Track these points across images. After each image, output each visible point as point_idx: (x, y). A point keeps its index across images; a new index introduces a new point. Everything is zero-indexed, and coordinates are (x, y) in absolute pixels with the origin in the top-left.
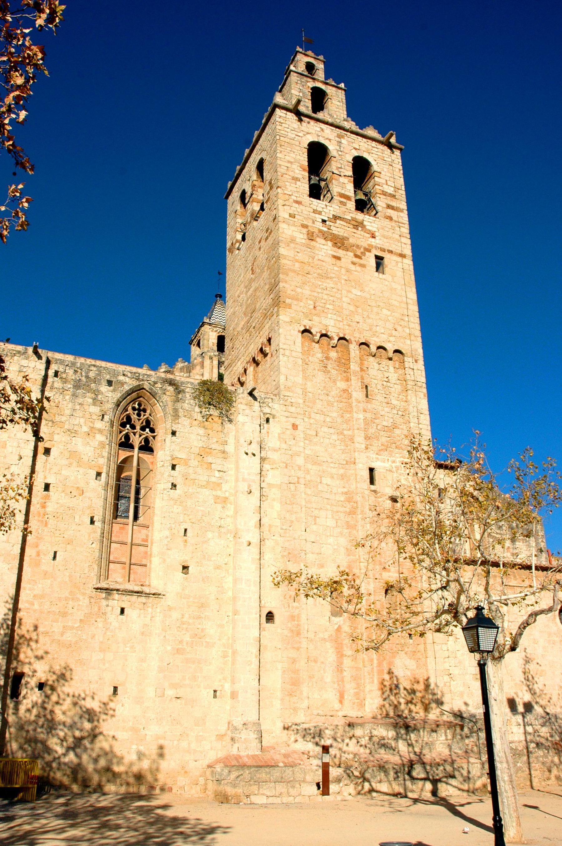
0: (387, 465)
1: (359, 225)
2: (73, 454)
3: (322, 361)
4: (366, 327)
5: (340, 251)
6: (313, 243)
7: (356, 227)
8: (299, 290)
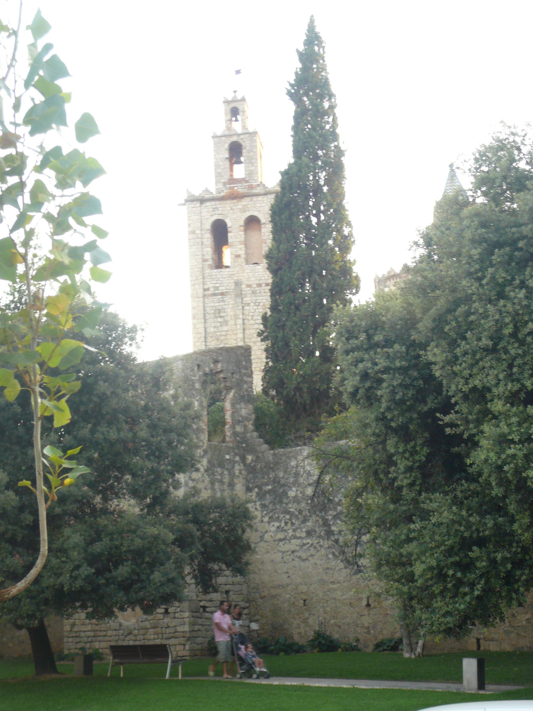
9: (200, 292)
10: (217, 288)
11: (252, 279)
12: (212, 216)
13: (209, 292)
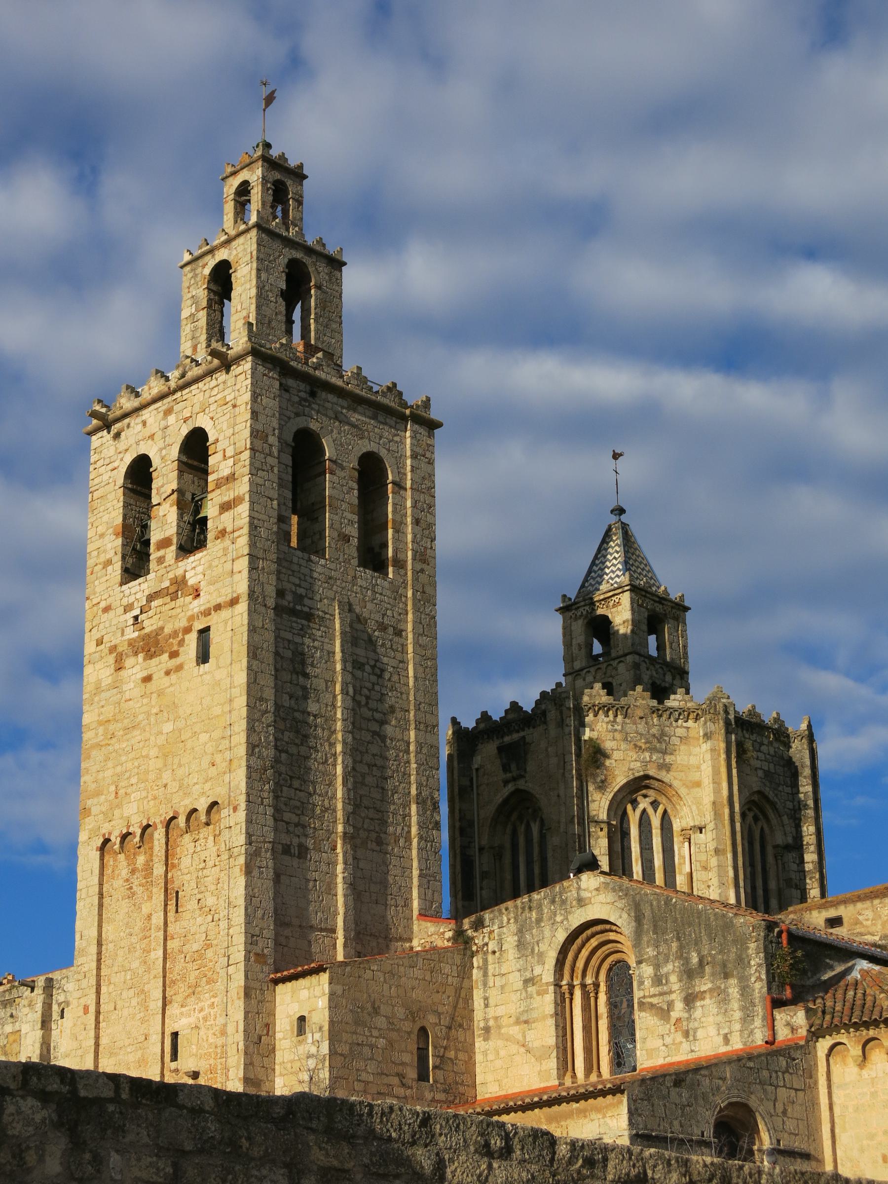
0: (192, 1020)
1: (179, 587)
3: (127, 880)
4: (173, 786)
5: (155, 661)
6: (122, 673)
8: (101, 775)
9: (271, 591)
10: (299, 598)
11: (370, 606)
12: (297, 415)
13: (285, 603)
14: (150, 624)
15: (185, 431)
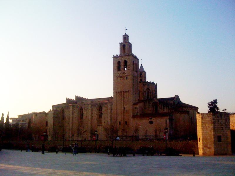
2: (95, 113)
7: (123, 73)
14: (121, 75)
15: (124, 60)
